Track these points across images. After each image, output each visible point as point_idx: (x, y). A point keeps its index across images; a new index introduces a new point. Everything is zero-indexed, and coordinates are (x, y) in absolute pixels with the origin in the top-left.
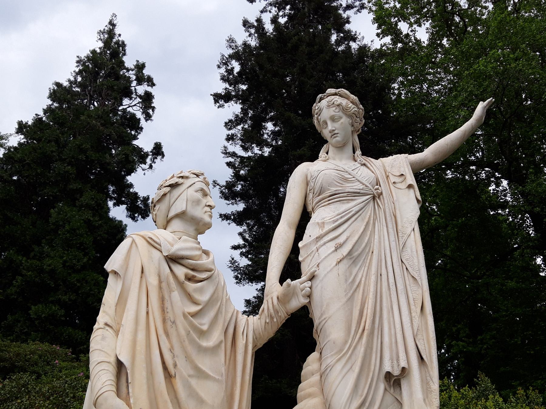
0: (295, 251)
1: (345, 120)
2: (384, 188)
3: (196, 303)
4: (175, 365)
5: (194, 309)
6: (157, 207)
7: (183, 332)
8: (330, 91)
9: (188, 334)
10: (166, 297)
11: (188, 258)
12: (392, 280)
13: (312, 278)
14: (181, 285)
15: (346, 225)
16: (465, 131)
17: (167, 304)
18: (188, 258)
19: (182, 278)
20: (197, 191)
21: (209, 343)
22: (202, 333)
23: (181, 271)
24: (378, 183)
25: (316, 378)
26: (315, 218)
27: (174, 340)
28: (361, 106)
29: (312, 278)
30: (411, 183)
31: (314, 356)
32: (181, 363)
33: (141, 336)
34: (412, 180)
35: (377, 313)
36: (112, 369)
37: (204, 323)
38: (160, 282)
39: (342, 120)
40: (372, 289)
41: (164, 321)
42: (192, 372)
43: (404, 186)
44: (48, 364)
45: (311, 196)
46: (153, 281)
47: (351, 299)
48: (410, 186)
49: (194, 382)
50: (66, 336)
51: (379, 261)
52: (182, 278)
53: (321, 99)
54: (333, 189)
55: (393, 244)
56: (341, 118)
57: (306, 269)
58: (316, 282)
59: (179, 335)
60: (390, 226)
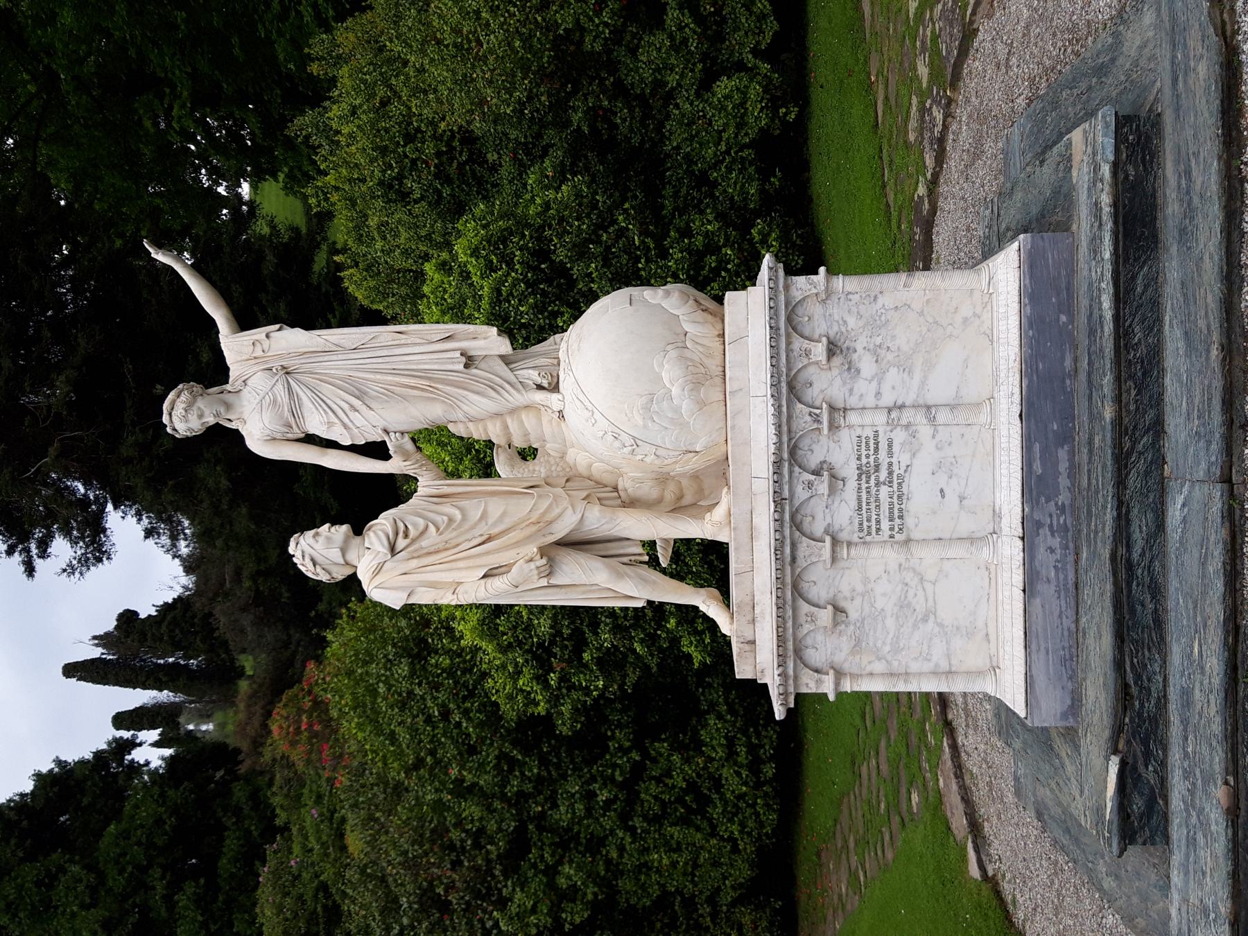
0: (353, 449)
1: (200, 403)
2: (276, 364)
3: (427, 527)
4: (481, 535)
5: (432, 528)
6: (335, 575)
7: (454, 534)
8: (165, 419)
9: (454, 529)
10: (425, 551)
11: (389, 539)
12: (380, 360)
13: (386, 432)
14: (414, 541)
15: (328, 402)
16: (190, 274)
17: (432, 549)
18: (389, 539)
19: (407, 541)
20: (317, 541)
21: (458, 515)
22: (451, 520)
23: (401, 543)
24: (270, 369)
25: (470, 425)
26: (312, 430)
27: (461, 540)
28: (180, 386)
29: (386, 432)
30: (264, 335)
31: (451, 427)
32: (477, 532)
33: (461, 564)
34: (261, 333)
35: (411, 374)
36: (489, 581)
37: (438, 519)
38: (413, 558)
39: (202, 407)
40: (390, 378)
41: (447, 549)
42: (484, 523)
43: (266, 343)
44: (297, 877)
45: (290, 436)
46: (414, 563)
47: (404, 398)
48: (267, 336)
49: (490, 521)
50: (236, 867)
51: (357, 370)
52: (407, 541)
53: (174, 429)
54: (287, 414)
55: (340, 357)
56: (199, 408)
57: (376, 437)
58: (390, 428)
59: (456, 537)
60: (321, 359)
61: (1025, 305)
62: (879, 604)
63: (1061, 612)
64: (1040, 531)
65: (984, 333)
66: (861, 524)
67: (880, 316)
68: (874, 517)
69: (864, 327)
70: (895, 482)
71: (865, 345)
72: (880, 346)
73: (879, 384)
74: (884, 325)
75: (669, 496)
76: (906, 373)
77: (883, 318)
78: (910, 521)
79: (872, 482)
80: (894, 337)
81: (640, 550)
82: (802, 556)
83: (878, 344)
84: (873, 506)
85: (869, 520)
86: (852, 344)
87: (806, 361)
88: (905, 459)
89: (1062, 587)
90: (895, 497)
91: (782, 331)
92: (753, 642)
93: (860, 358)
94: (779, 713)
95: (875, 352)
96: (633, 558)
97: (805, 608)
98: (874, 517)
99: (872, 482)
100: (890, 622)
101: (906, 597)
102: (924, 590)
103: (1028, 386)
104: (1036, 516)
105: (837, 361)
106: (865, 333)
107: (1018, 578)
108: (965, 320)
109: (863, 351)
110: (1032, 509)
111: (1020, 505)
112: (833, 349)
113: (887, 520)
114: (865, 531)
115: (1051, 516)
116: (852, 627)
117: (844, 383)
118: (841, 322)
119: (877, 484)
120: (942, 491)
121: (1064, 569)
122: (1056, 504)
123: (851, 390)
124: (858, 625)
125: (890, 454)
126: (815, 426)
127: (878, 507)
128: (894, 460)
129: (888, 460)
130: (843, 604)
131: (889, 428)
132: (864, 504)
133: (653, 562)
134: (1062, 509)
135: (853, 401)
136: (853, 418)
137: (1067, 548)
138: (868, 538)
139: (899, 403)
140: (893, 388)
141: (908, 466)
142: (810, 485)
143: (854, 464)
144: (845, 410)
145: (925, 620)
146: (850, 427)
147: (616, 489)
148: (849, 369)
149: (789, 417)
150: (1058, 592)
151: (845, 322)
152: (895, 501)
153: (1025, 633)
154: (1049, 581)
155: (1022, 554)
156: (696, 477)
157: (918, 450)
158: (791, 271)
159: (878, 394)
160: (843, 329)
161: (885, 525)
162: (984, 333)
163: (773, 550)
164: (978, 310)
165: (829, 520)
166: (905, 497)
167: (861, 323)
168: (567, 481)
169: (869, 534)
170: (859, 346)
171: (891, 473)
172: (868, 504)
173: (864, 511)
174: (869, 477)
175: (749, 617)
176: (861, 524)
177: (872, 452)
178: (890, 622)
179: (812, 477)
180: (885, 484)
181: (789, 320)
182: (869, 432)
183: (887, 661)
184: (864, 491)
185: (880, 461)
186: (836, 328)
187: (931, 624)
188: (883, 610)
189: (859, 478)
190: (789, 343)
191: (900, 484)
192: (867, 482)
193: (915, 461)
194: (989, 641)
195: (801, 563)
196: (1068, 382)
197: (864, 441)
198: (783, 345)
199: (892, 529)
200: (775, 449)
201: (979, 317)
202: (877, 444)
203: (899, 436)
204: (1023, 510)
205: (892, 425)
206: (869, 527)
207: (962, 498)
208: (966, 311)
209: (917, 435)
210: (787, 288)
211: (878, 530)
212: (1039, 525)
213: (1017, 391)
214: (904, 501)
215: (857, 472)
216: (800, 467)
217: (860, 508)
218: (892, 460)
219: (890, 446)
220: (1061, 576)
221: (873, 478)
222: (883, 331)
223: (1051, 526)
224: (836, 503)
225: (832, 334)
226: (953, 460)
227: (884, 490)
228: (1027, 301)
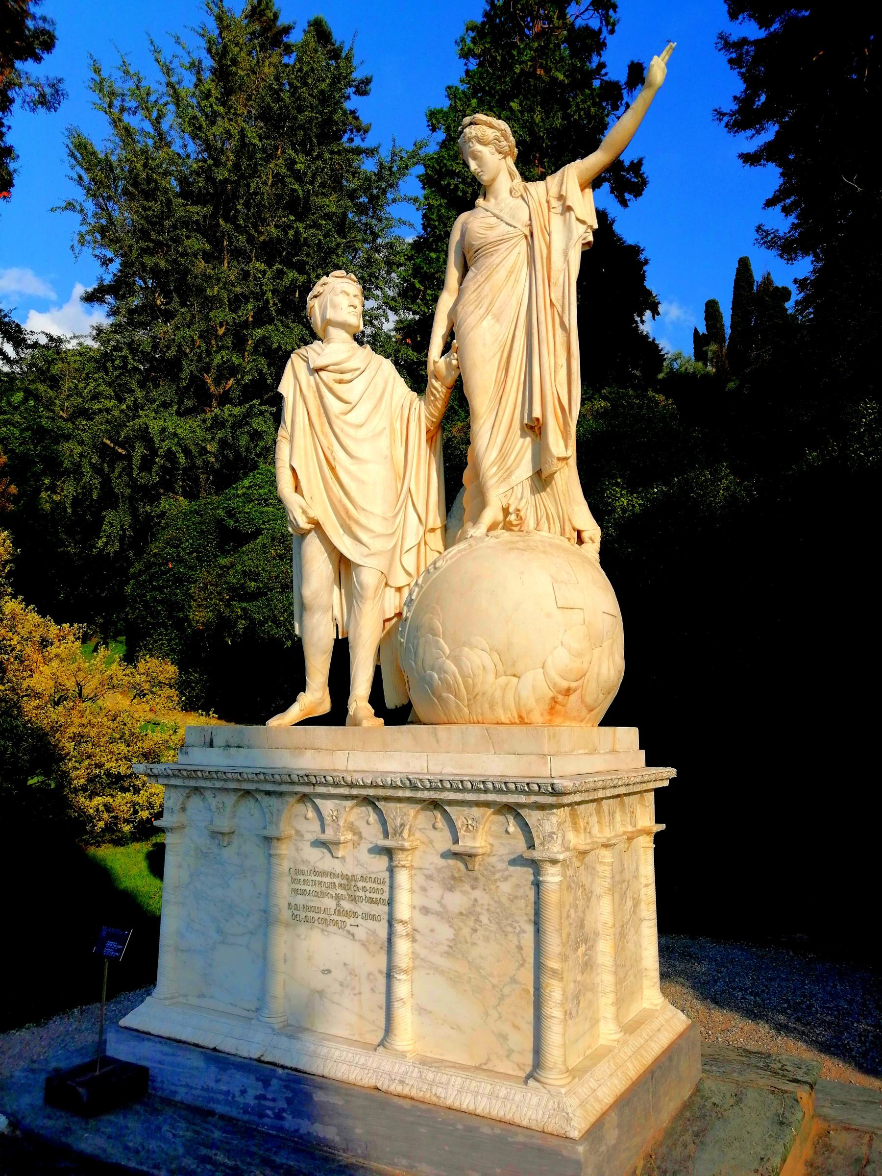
63: (191, 1088)
65: (489, 1060)
67: (511, 925)
68: (308, 888)
69: (499, 902)
70: (339, 918)
71: (480, 902)
72: (477, 920)
73: (437, 914)
74: (501, 928)
77: (509, 929)
79: (340, 891)
80: (487, 939)
82: (271, 803)
84: (317, 888)
88: (360, 933)
89: (211, 1095)
92: (211, 745)
93: (464, 893)
95: (470, 913)
99: (340, 891)
103: (401, 1108)
104: (274, 1082)
106: (492, 902)
107: (228, 1045)
108: (504, 1037)
109: (473, 898)
110: (280, 1079)
111: (288, 1064)
113: (304, 902)
115: (274, 1100)
117: (439, 870)
118: (506, 873)
119: (338, 898)
120: (329, 971)
121: (227, 1103)
122: (284, 1110)
128: (359, 921)
134: (279, 1116)
137: (245, 1112)
140: (432, 931)
141: (353, 935)
143: (358, 871)
145: (219, 931)
148: (453, 878)
150: (207, 1089)
151: (506, 879)
152: (321, 916)
153: (180, 1041)
155: (246, 1055)
157: (368, 950)
160: (497, 876)
162: (489, 1060)
163: (262, 770)
166: (325, 928)
167: (504, 900)
170: (477, 894)
171: (347, 914)
174: (344, 889)
175: (231, 742)
177: (368, 895)
184: (331, 881)
185: (359, 903)
188: (228, 886)
189: (344, 876)
191: (336, 923)
193: (357, 945)
194: (199, 997)
196: (404, 1162)
197: (380, 887)
204: (283, 1067)
212: (266, 1083)
213: (406, 1091)
214: (321, 926)
215: (350, 875)
218: (360, 918)
220: (221, 1097)
221: (343, 892)
222: (493, 927)
223: (263, 1097)
226: (356, 991)
227: (330, 903)
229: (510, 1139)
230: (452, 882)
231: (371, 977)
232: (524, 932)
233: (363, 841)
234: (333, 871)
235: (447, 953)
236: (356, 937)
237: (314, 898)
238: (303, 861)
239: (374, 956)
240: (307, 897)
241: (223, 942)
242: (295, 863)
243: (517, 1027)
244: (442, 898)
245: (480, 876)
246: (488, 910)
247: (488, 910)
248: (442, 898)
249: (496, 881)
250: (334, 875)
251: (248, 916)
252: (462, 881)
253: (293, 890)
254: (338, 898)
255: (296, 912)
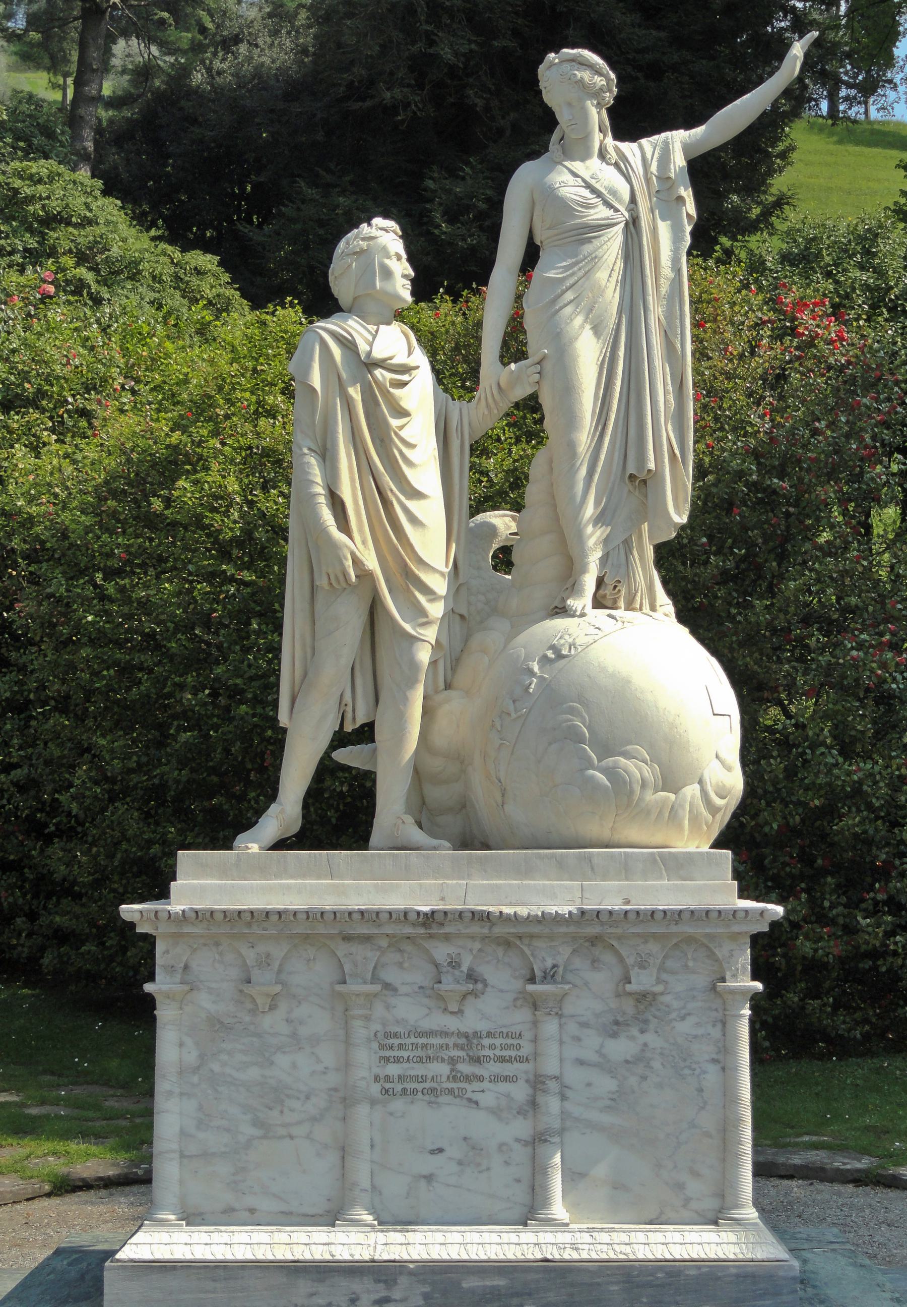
61: (699, 1268)
62: (283, 1060)
64: (382, 1285)
65: (662, 1213)
66: (396, 1035)
67: (689, 1067)
68: (405, 1054)
70: (454, 1085)
72: (648, 1066)
75: (435, 764)
76: (608, 1103)
78: (398, 1105)
81: (361, 720)
83: (653, 1064)
84: (419, 1053)
85: (401, 1047)
86: (652, 1026)
87: (630, 961)
88: (488, 1099)
90: (434, 1085)
91: (674, 929)
93: (632, 1038)
94: (129, 911)
95: (641, 1059)
96: (349, 709)
97: (278, 952)
98: (405, 1054)
100: (253, 1073)
101: (288, 1096)
102: (299, 1123)
105: (629, 1006)
112: (644, 998)
113: (400, 1072)
114: (386, 1042)
116: (247, 1019)
118: (684, 1012)
119: (453, 1061)
120: (441, 1150)
123: (584, 1025)
124: (252, 1028)
125: (496, 1079)
126: (538, 974)
127: (420, 1060)
128: (486, 1084)
129: (486, 1075)
130: (283, 1006)
131: (532, 1077)
132: (424, 1040)
133: (341, 739)
135: (572, 1028)
136: (550, 1027)
138: (375, 1045)
139: (569, 1093)
140: (589, 1085)
141: (476, 1103)
142: (454, 964)
143: (482, 1026)
144: (560, 1016)
145: (257, 1123)
146: (535, 1023)
147: (448, 686)
149: (551, 937)
151: (683, 1018)
152: (427, 1085)
154: (312, 1295)
156: (464, 805)
158: (756, 940)
159: (581, 1062)
160: (674, 1015)
161: (393, 1070)
162: (662, 1213)
164: (694, 1205)
165: (403, 989)
166: (433, 1099)
168: (462, 617)
169: (382, 1047)
171: (468, 1079)
172: (424, 1046)
173: (413, 1040)
174: (462, 1049)
176: (396, 1035)
177: (498, 1053)
178: (253, 1073)
179: (465, 968)
180: (452, 1070)
181: (690, 940)
182: (527, 1049)
183: (198, 1068)
185: (486, 1065)
186: (676, 1004)
187: (249, 1131)
188: (272, 1063)
189: (459, 1034)
190: (654, 936)
191: (451, 1091)
192: (456, 1045)
195: (342, 949)
197: (515, 1042)
198: (654, 929)
199: (387, 1078)
200: (508, 915)
201: (684, 1206)
202: (510, 1060)
203: (520, 1092)
205: (537, 1083)
206: (391, 1048)
207: (429, 1178)
208: (694, 1187)
209: (521, 1118)
210: (734, 937)
211: (387, 1060)
214: (427, 1098)
216: (480, 950)
217: (419, 1035)
219: (506, 1079)
221: (461, 1053)
224: (426, 1001)
225: (667, 999)
227: (443, 1069)
228: (704, 1270)
229: (720, 1274)
230: (615, 1028)
231: (504, 1148)
232: (705, 1072)
233: (489, 989)
234: (445, 1029)
235: (609, 1107)
236: (482, 1104)
237: (415, 1065)
238: (398, 1022)
239: (507, 1123)
240: (406, 1065)
241: (264, 1137)
242: (384, 1025)
243: (695, 1174)
244: (602, 1046)
245: (651, 1018)
246: (661, 1054)
247: (661, 1054)
248: (602, 1046)
249: (671, 1021)
250: (446, 1034)
251: (308, 1098)
252: (628, 1025)
253: (382, 1058)
254: (453, 1061)
255: (388, 1086)
